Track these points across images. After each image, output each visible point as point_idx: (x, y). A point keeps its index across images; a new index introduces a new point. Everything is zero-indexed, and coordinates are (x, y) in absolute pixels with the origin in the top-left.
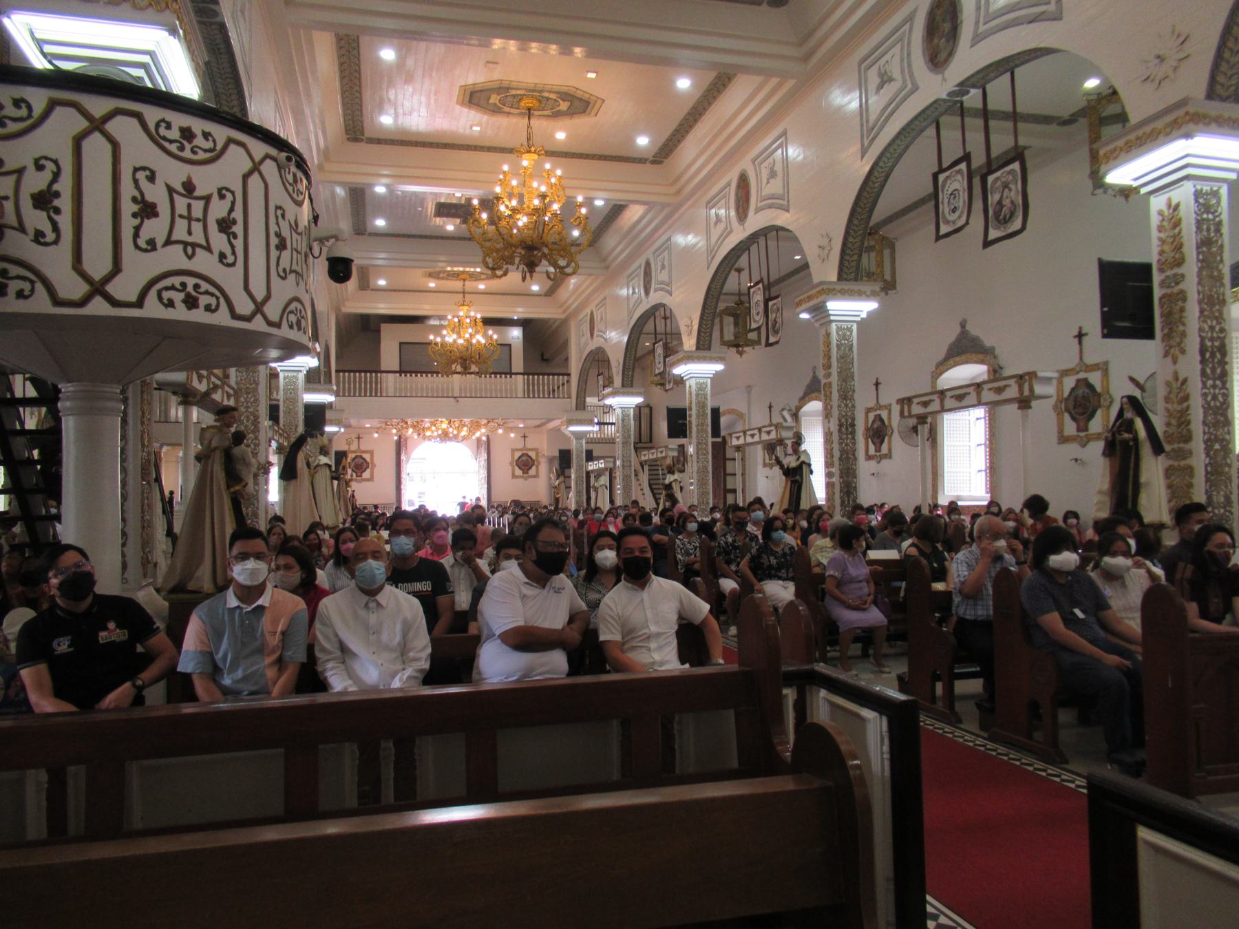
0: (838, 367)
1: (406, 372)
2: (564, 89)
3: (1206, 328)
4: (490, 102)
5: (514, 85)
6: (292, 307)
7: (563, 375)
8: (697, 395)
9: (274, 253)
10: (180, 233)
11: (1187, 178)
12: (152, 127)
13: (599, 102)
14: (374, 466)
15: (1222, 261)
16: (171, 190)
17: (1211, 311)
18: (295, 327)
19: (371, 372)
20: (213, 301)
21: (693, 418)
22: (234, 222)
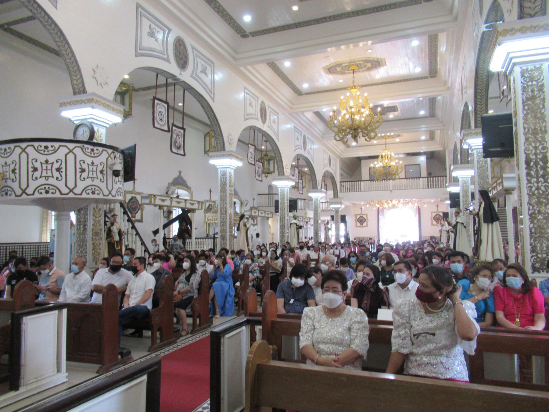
0: (478, 172)
2: (363, 59)
3: (531, 148)
5: (342, 62)
7: (443, 176)
9: (78, 174)
10: (44, 174)
14: (368, 220)
16: (41, 163)
17: (535, 137)
18: (91, 194)
19: (359, 181)
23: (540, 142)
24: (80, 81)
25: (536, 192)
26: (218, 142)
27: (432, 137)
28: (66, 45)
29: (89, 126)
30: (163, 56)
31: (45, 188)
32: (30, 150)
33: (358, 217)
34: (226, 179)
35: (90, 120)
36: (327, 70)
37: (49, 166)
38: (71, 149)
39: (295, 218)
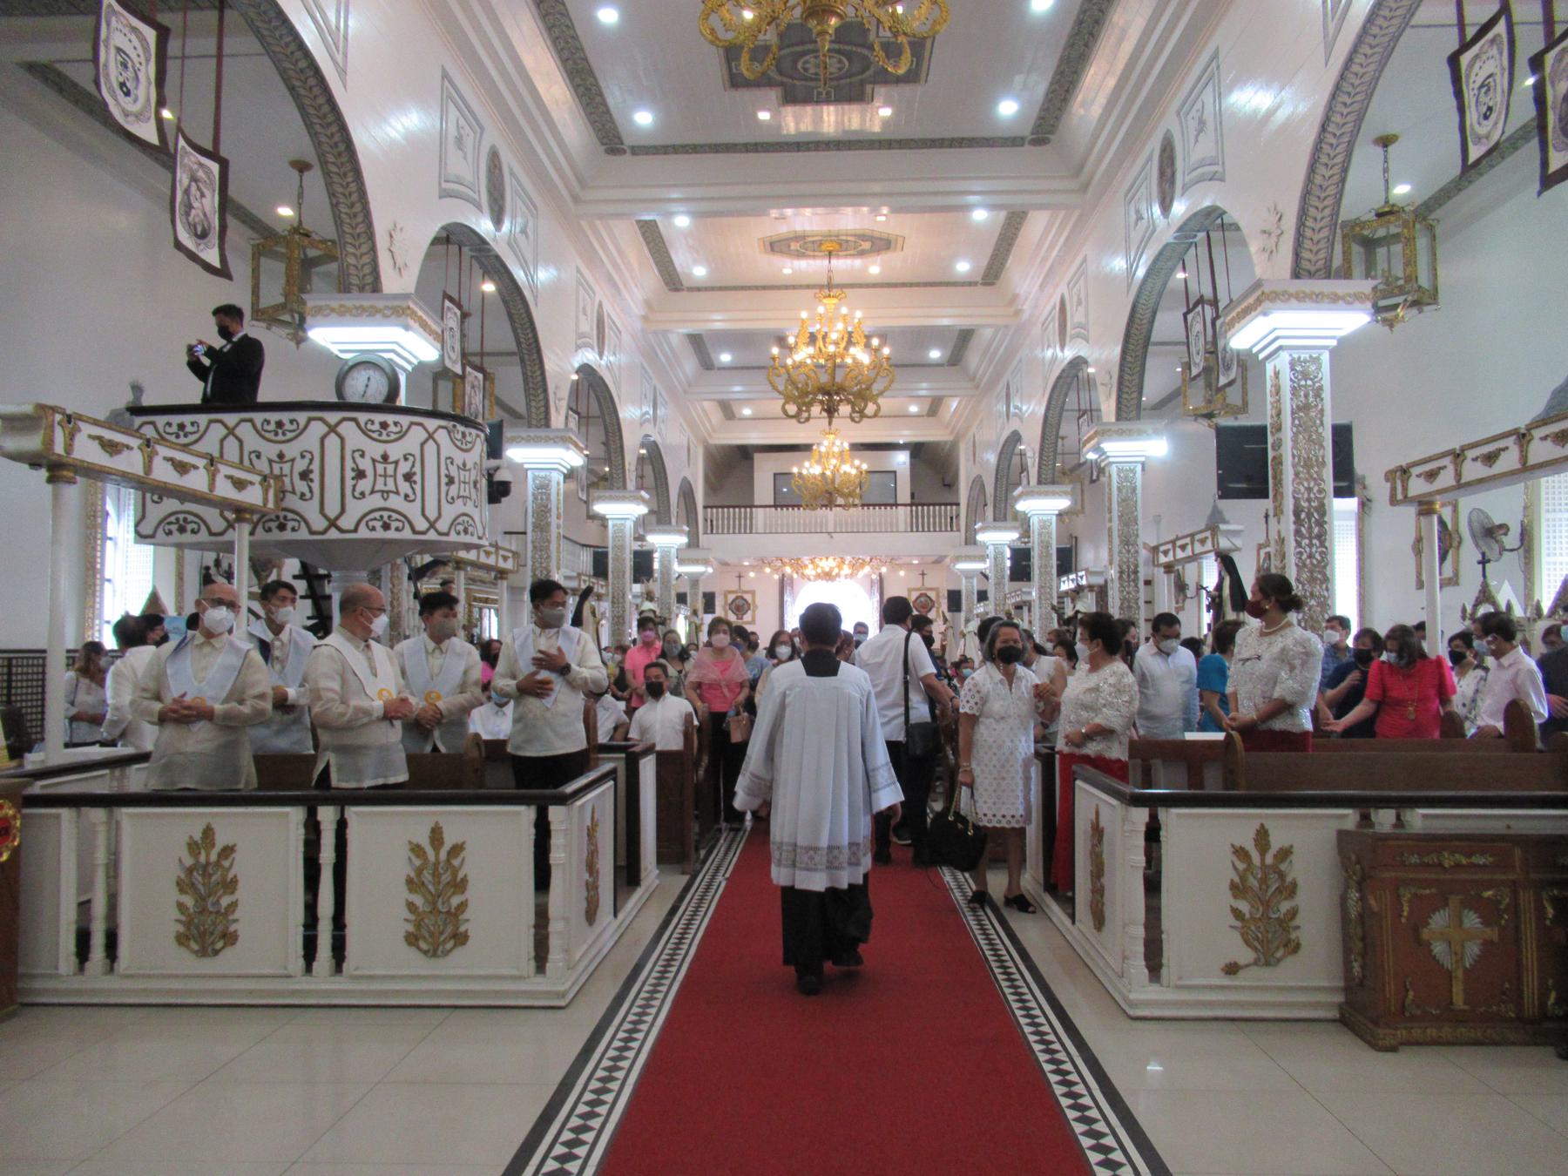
1: (782, 507)
4: (792, 247)
6: (460, 520)
7: (951, 504)
8: (1040, 534)
9: (444, 488)
10: (380, 486)
11: (1280, 348)
12: (363, 425)
13: (900, 241)
14: (756, 607)
15: (1322, 424)
16: (374, 461)
17: (1308, 472)
19: (745, 507)
20: (400, 525)
21: (1036, 561)
22: (415, 474)
23: (1315, 479)
24: (366, 259)
25: (1308, 561)
26: (533, 404)
27: (935, 406)
28: (350, 174)
29: (387, 369)
30: (471, 193)
31: (382, 517)
32: (348, 429)
33: (731, 597)
34: (548, 499)
35: (386, 356)
36: (768, 244)
37: (390, 468)
38: (431, 430)
39: (649, 596)
